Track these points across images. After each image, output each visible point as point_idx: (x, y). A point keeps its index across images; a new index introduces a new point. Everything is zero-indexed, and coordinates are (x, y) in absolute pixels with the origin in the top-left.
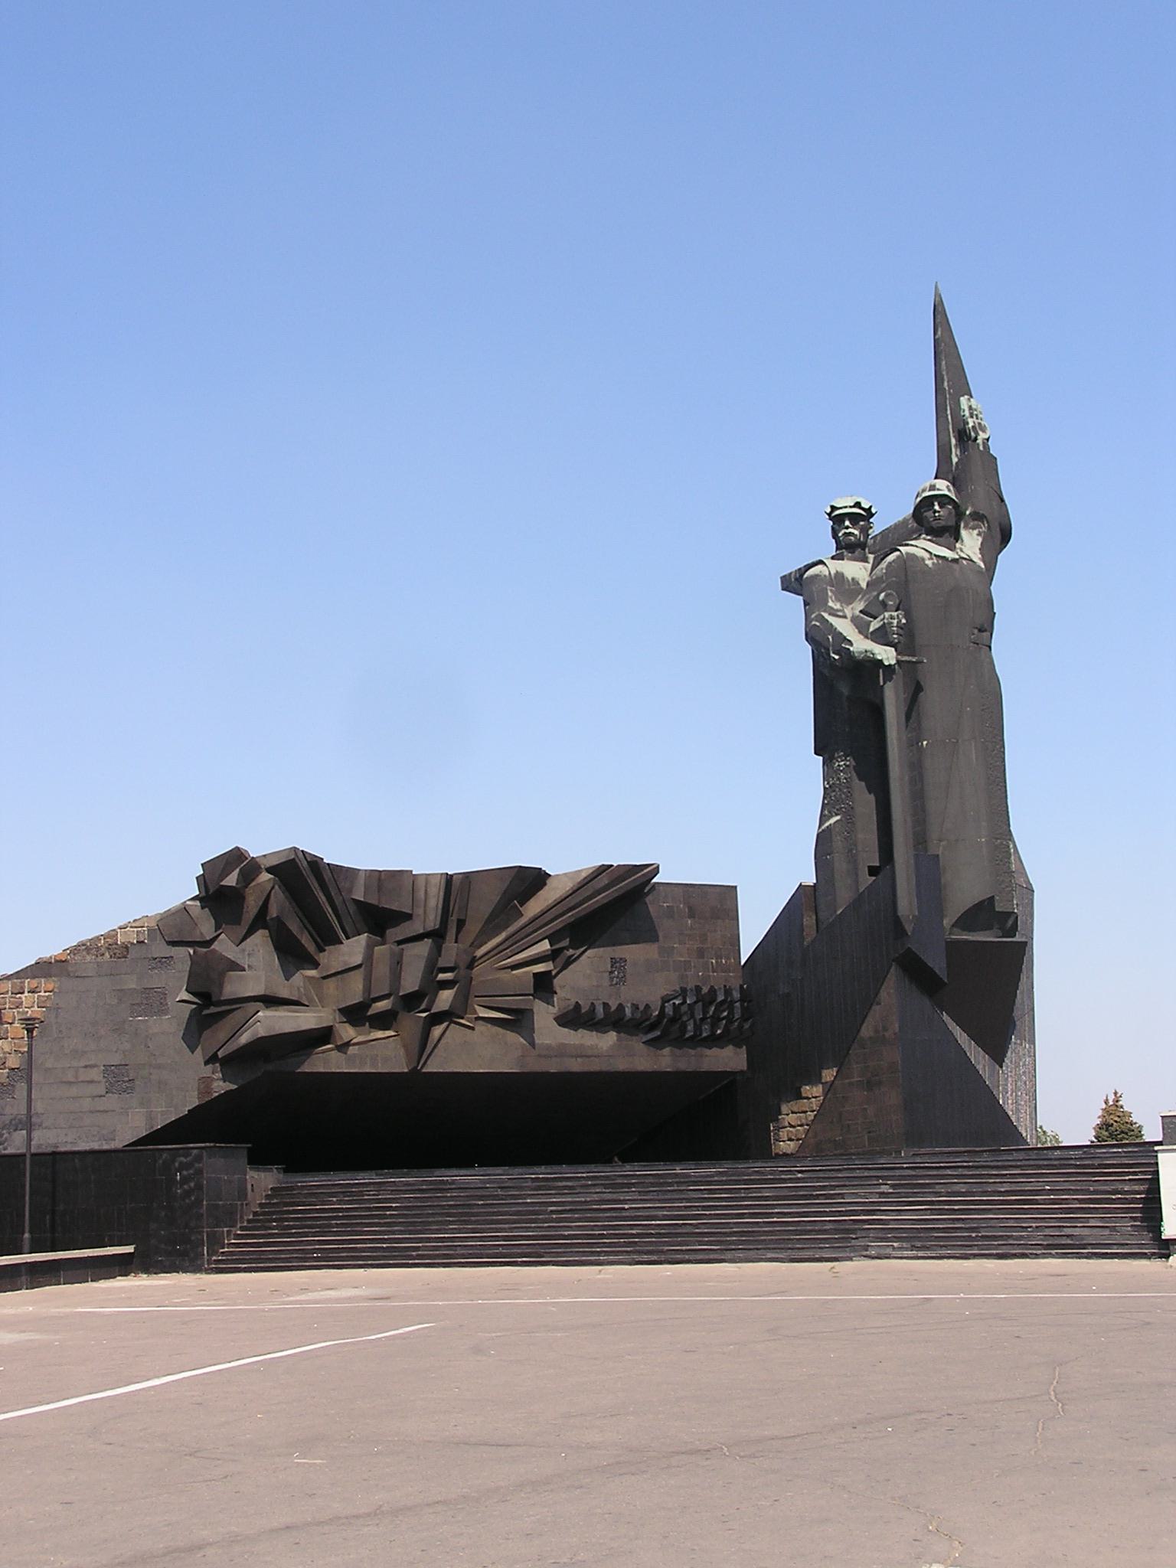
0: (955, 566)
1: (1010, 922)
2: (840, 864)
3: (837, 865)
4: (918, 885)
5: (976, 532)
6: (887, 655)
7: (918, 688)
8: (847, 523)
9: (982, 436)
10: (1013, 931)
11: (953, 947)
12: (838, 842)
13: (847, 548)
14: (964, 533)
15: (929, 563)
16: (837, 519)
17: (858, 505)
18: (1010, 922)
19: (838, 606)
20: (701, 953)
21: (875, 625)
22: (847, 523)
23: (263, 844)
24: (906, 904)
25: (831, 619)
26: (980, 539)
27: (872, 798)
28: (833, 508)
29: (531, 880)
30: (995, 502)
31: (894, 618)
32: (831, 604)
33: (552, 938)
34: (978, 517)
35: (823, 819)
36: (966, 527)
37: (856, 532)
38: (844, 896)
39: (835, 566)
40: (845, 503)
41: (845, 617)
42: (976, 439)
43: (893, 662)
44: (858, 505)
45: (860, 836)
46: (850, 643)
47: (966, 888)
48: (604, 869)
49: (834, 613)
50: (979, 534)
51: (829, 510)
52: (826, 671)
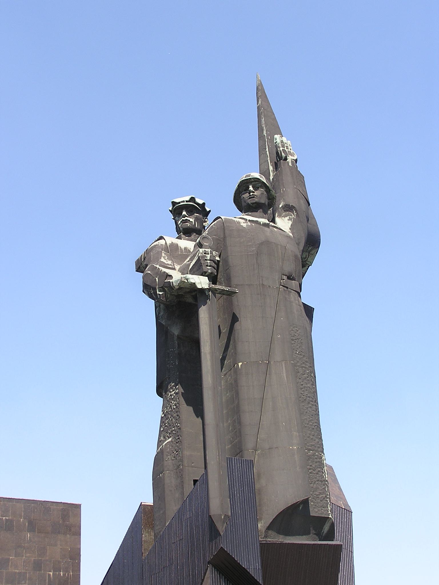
0: (266, 229)
1: (326, 528)
2: (170, 479)
3: (167, 481)
4: (231, 487)
5: (288, 217)
6: (202, 282)
7: (235, 319)
8: (184, 213)
9: (290, 158)
10: (330, 535)
11: (266, 549)
12: (169, 461)
13: (186, 232)
14: (277, 219)
15: (244, 225)
16: (177, 210)
17: (192, 199)
18: (326, 528)
19: (169, 262)
20: (38, 566)
22: (184, 213)
24: (218, 504)
26: (290, 223)
27: (191, 409)
28: (174, 203)
30: (303, 202)
31: (208, 253)
32: (162, 260)
34: (288, 208)
35: (160, 442)
36: (280, 216)
37: (191, 220)
38: (173, 507)
39: (171, 239)
40: (183, 199)
41: (174, 269)
42: (286, 159)
43: (206, 286)
44: (192, 199)
45: (187, 453)
46: (171, 276)
47: (279, 492)
52: (163, 322)
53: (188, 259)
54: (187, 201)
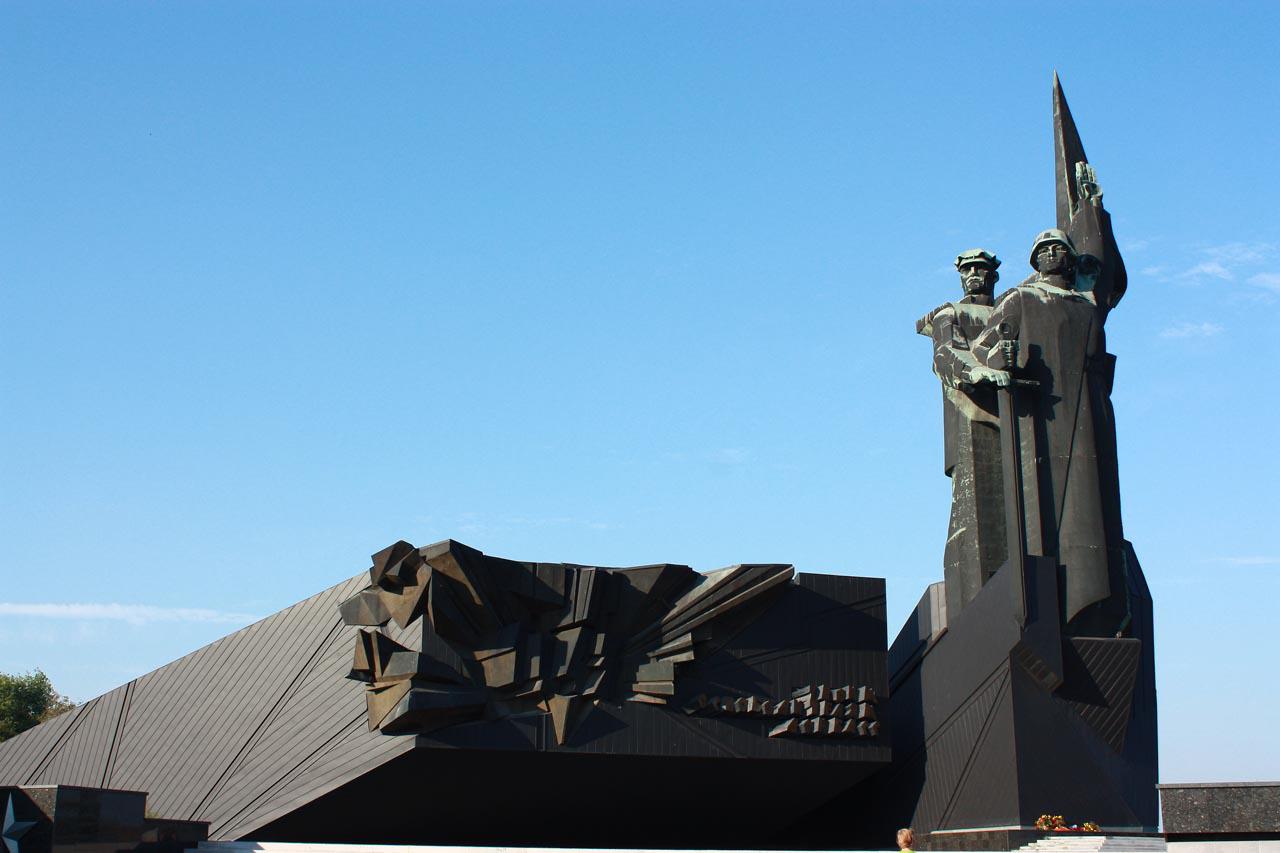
5: (1089, 277)
6: (1000, 377)
15: (1044, 300)
17: (982, 255)
21: (992, 352)
23: (425, 537)
25: (953, 351)
26: (1094, 283)
28: (961, 259)
29: (679, 578)
32: (955, 338)
33: (692, 631)
35: (951, 531)
36: (1082, 272)
40: (972, 253)
41: (968, 349)
48: (745, 569)
49: (956, 346)
50: (1093, 278)
51: (957, 262)
53: (981, 338)
54: (976, 257)
